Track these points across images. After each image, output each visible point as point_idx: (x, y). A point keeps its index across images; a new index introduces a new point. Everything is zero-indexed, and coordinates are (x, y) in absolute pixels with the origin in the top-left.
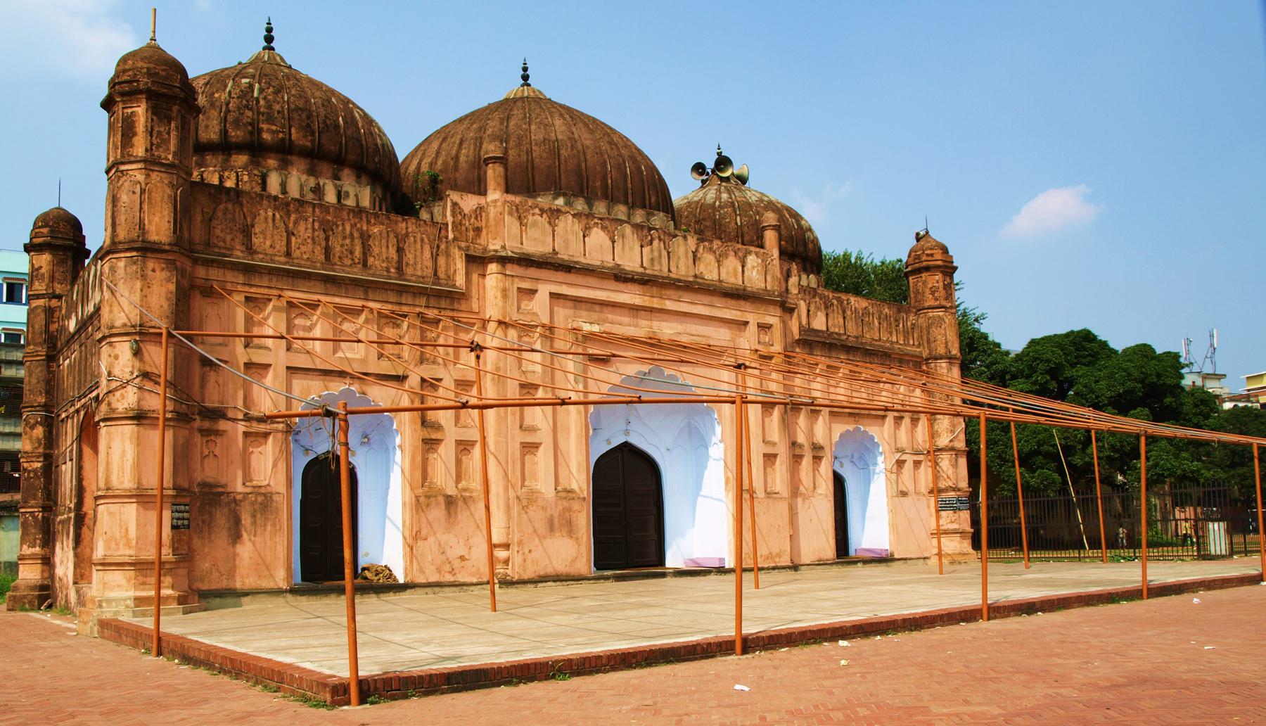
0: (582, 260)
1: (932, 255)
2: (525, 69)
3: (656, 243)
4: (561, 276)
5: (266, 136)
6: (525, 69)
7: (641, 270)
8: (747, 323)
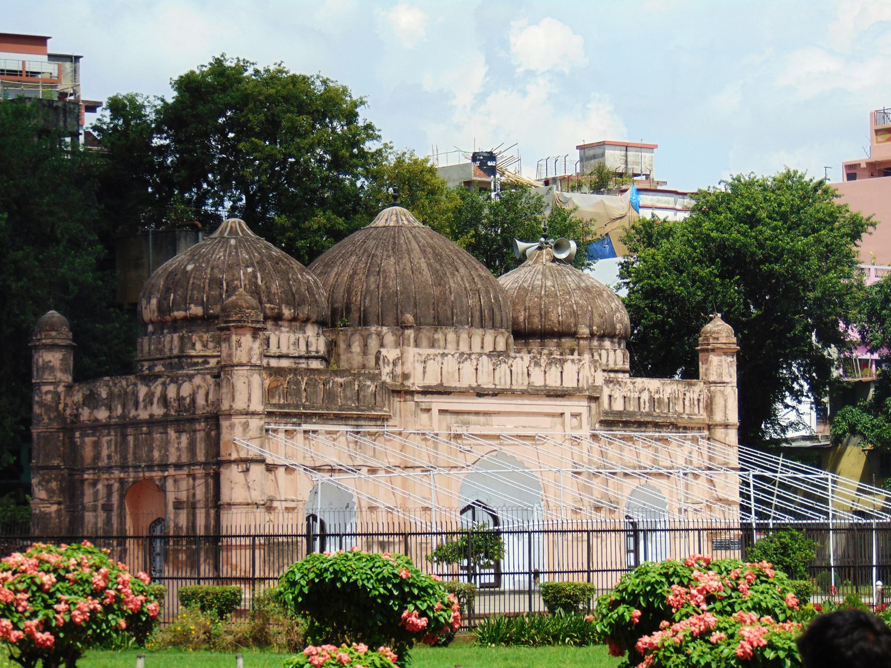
0: (458, 385)
1: (717, 339)
3: (503, 365)
5: (268, 311)
7: (493, 386)
8: (562, 414)
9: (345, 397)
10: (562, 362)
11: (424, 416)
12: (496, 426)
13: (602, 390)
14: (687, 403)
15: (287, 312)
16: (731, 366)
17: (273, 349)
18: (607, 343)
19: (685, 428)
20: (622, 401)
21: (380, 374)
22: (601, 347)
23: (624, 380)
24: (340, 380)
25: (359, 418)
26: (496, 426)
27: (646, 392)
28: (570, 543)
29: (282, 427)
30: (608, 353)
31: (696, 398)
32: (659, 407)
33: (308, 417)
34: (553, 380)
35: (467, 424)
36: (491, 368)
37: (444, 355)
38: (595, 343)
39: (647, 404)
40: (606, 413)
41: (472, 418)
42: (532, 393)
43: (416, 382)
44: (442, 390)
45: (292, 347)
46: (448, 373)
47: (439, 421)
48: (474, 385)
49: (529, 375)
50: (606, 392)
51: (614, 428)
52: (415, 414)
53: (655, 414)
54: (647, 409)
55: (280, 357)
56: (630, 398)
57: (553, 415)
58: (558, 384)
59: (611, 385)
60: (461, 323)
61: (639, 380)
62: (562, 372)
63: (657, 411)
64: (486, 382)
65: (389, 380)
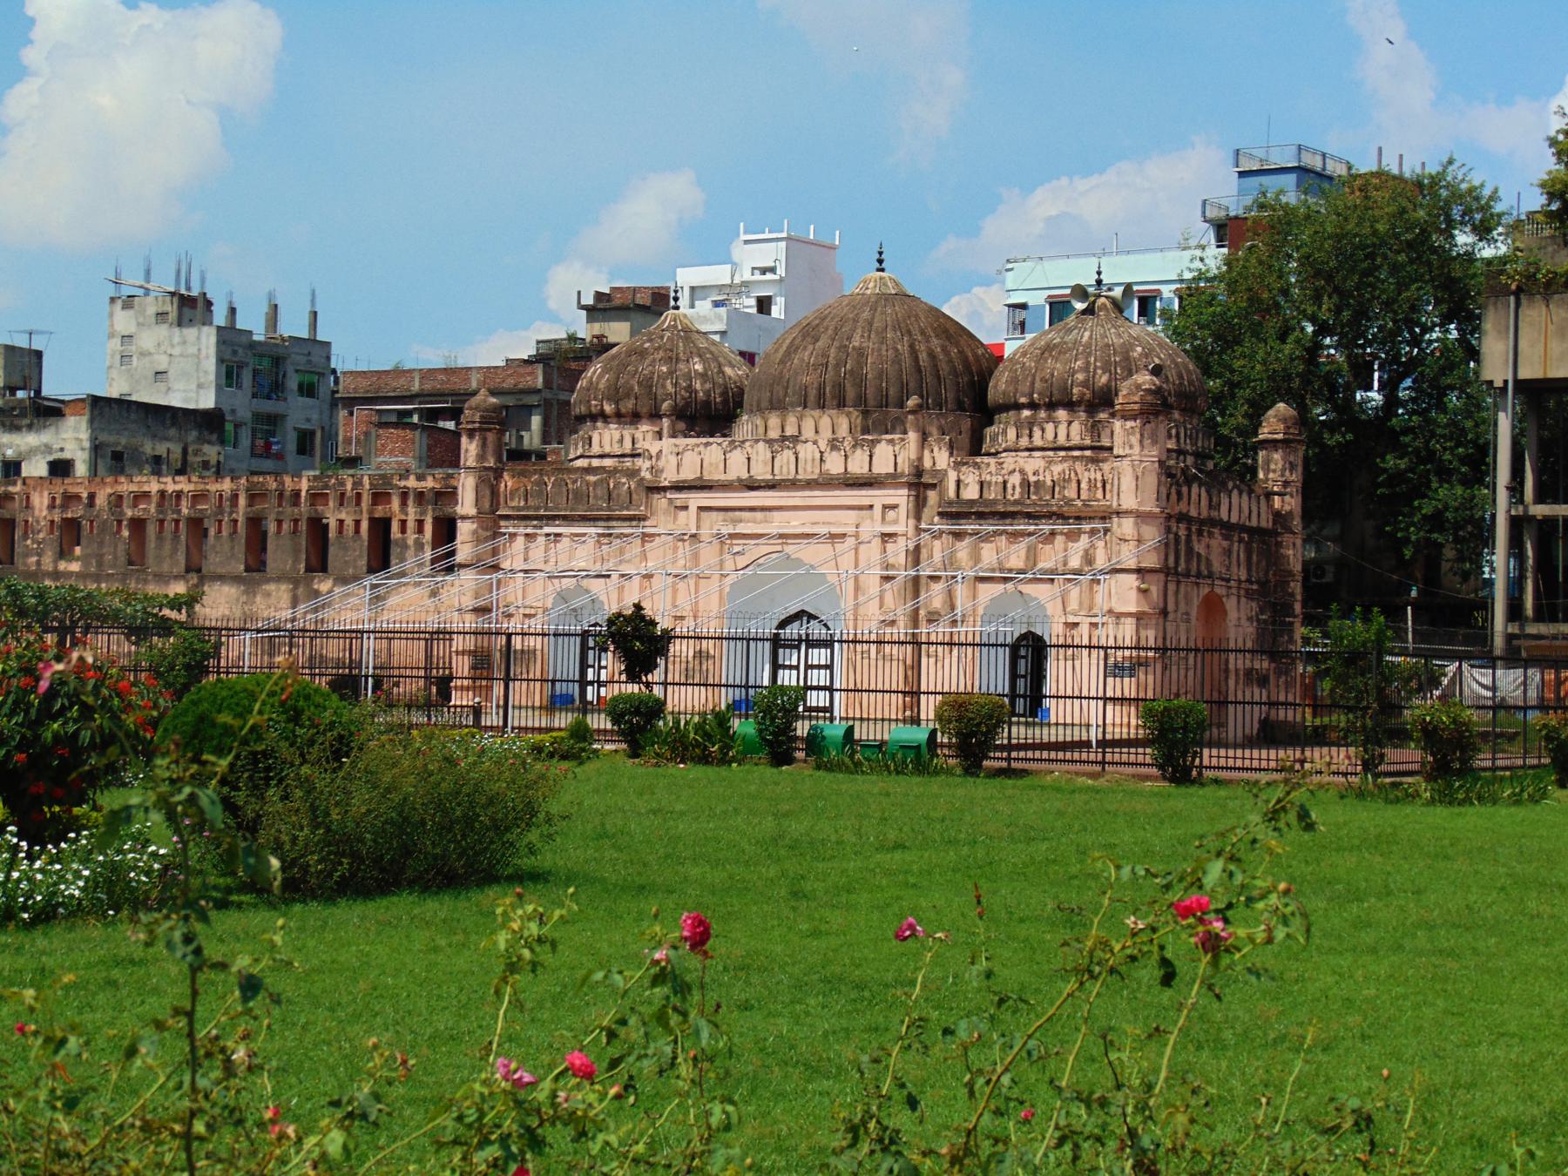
0: (722, 477)
2: (881, 253)
3: (786, 451)
6: (881, 253)
8: (871, 507)
9: (595, 497)
10: (873, 443)
11: (682, 514)
12: (778, 523)
14: (1084, 485)
15: (608, 408)
16: (1133, 434)
17: (596, 449)
18: (1062, 414)
19: (1078, 518)
20: (977, 487)
21: (639, 470)
22: (1050, 419)
24: (592, 478)
25: (609, 518)
26: (778, 523)
28: (873, 663)
29: (522, 530)
31: (1099, 477)
36: (769, 455)
37: (707, 444)
38: (1043, 414)
39: (1018, 490)
40: (950, 503)
43: (669, 477)
44: (698, 483)
45: (616, 446)
48: (745, 475)
50: (952, 476)
52: (666, 512)
54: (1017, 496)
55: (601, 456)
57: (860, 508)
58: (865, 470)
59: (964, 469)
60: (793, 405)
64: (761, 472)
65: (646, 475)
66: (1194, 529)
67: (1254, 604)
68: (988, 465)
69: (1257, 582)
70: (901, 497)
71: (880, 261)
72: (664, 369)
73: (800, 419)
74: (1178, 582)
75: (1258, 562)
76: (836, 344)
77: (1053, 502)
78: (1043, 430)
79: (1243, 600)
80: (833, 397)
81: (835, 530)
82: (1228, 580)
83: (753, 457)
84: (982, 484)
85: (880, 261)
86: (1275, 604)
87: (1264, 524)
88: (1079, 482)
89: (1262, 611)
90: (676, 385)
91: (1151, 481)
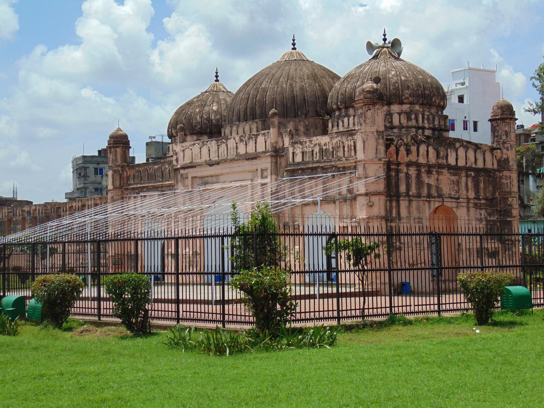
2: (294, 40)
4: (194, 169)
6: (294, 40)
7: (217, 159)
13: (288, 150)
14: (346, 149)
20: (301, 155)
23: (305, 140)
24: (156, 167)
27: (317, 146)
30: (349, 120)
31: (352, 144)
32: (326, 156)
33: (141, 189)
34: (251, 149)
35: (206, 183)
36: (217, 147)
39: (318, 154)
41: (210, 179)
42: (239, 158)
44: (190, 165)
46: (195, 155)
47: (192, 184)
49: (237, 148)
50: (291, 150)
51: (295, 174)
53: (322, 161)
56: (306, 152)
59: (296, 146)
61: (314, 138)
62: (256, 143)
63: (325, 158)
66: (423, 170)
67: (483, 212)
68: (306, 142)
69: (486, 199)
70: (266, 163)
71: (294, 44)
72: (197, 110)
73: (238, 128)
74: (410, 201)
75: (485, 188)
76: (255, 87)
77: (333, 159)
78: (343, 122)
79: (472, 210)
80: (251, 115)
81: (243, 183)
82: (458, 198)
83: (211, 149)
84: (303, 153)
85: (294, 44)
86: (500, 211)
87: (489, 165)
88: (344, 147)
89: (490, 215)
90: (201, 117)
91: (372, 143)
